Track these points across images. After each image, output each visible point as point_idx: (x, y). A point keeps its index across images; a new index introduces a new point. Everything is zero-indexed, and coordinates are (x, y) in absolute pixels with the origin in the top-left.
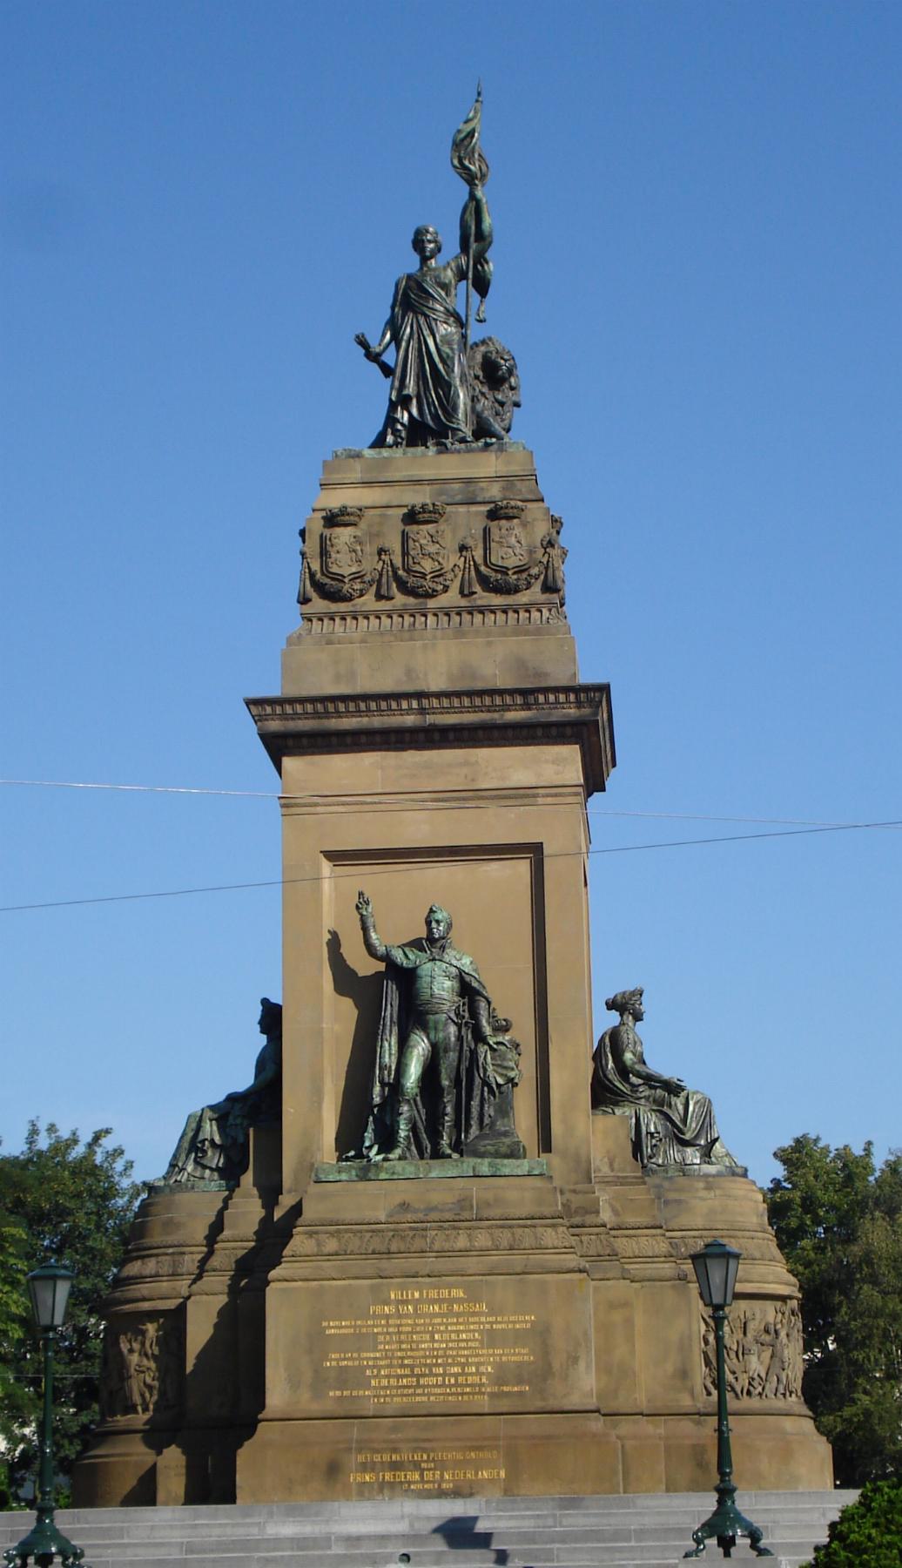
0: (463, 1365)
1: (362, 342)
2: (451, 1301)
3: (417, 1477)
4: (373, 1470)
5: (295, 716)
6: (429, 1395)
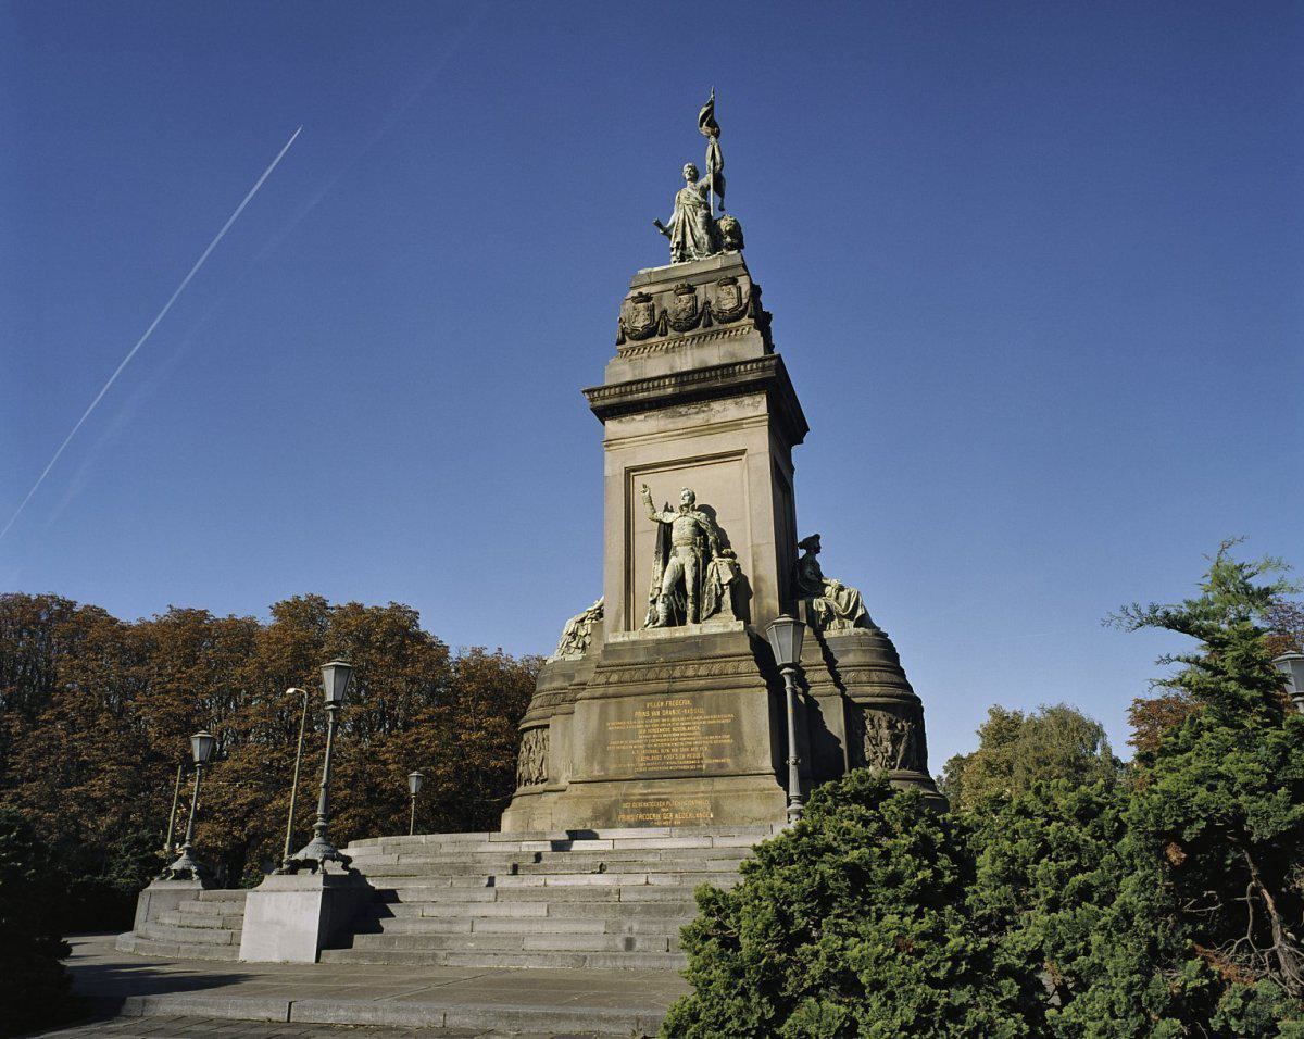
0: (690, 747)
1: (659, 224)
2: (683, 707)
3: (658, 816)
4: (632, 812)
5: (610, 396)
6: (669, 766)
